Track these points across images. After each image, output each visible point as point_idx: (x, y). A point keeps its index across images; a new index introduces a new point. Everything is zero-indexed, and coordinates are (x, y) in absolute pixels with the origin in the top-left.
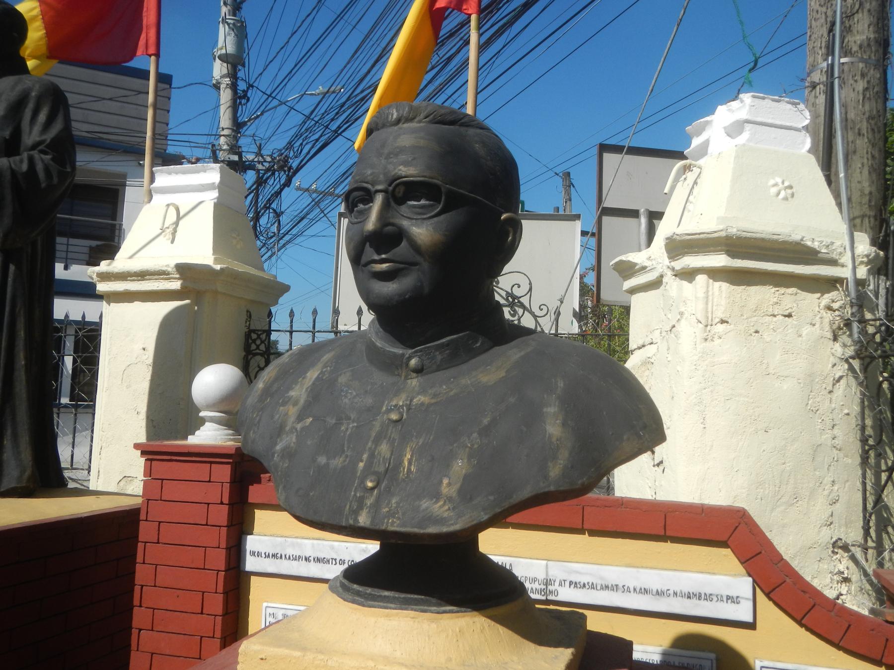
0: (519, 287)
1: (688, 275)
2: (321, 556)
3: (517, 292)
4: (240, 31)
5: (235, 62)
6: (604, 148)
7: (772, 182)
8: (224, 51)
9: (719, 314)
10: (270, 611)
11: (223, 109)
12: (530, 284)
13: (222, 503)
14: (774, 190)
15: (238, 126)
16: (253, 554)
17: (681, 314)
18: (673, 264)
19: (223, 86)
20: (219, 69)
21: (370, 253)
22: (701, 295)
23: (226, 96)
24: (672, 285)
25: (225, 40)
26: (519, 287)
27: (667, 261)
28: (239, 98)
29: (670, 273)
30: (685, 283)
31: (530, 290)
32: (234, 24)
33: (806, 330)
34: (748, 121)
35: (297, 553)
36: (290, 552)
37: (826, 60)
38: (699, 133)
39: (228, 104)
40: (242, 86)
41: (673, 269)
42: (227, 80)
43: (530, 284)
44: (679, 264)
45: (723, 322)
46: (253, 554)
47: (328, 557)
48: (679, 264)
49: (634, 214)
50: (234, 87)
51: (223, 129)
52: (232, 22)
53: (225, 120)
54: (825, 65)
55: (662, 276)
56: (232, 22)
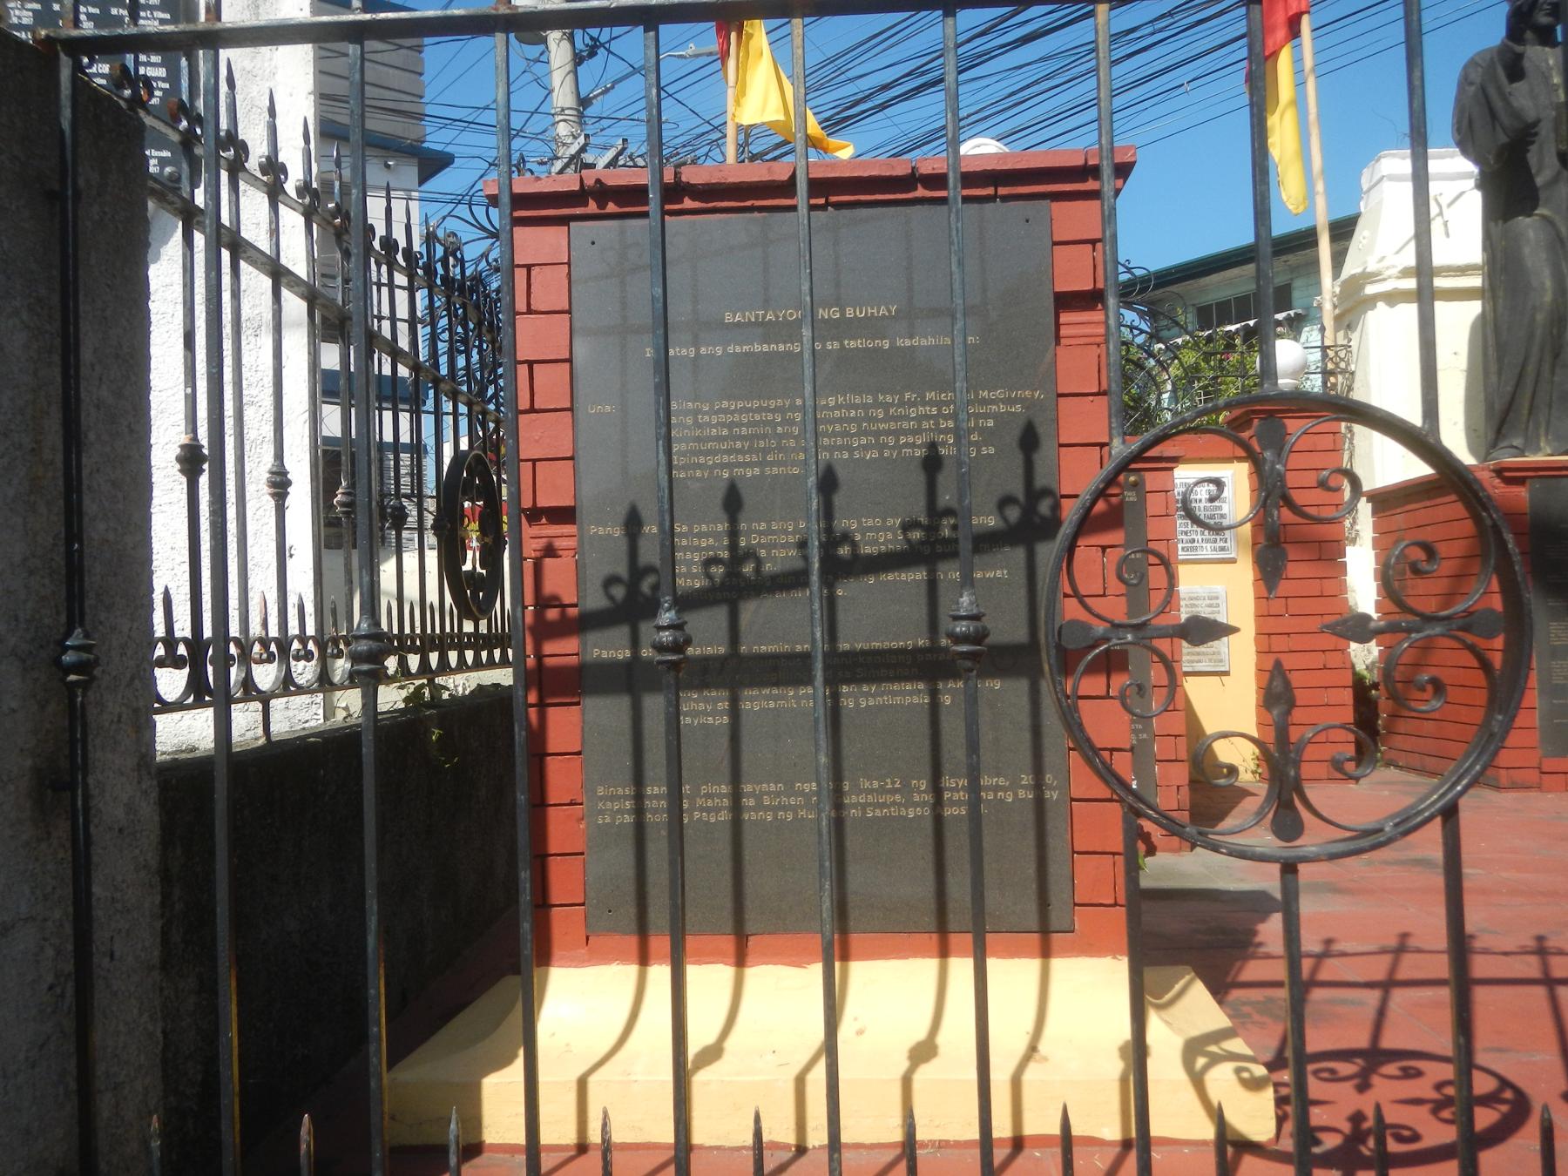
15: (584, 102)
53: (563, 97)
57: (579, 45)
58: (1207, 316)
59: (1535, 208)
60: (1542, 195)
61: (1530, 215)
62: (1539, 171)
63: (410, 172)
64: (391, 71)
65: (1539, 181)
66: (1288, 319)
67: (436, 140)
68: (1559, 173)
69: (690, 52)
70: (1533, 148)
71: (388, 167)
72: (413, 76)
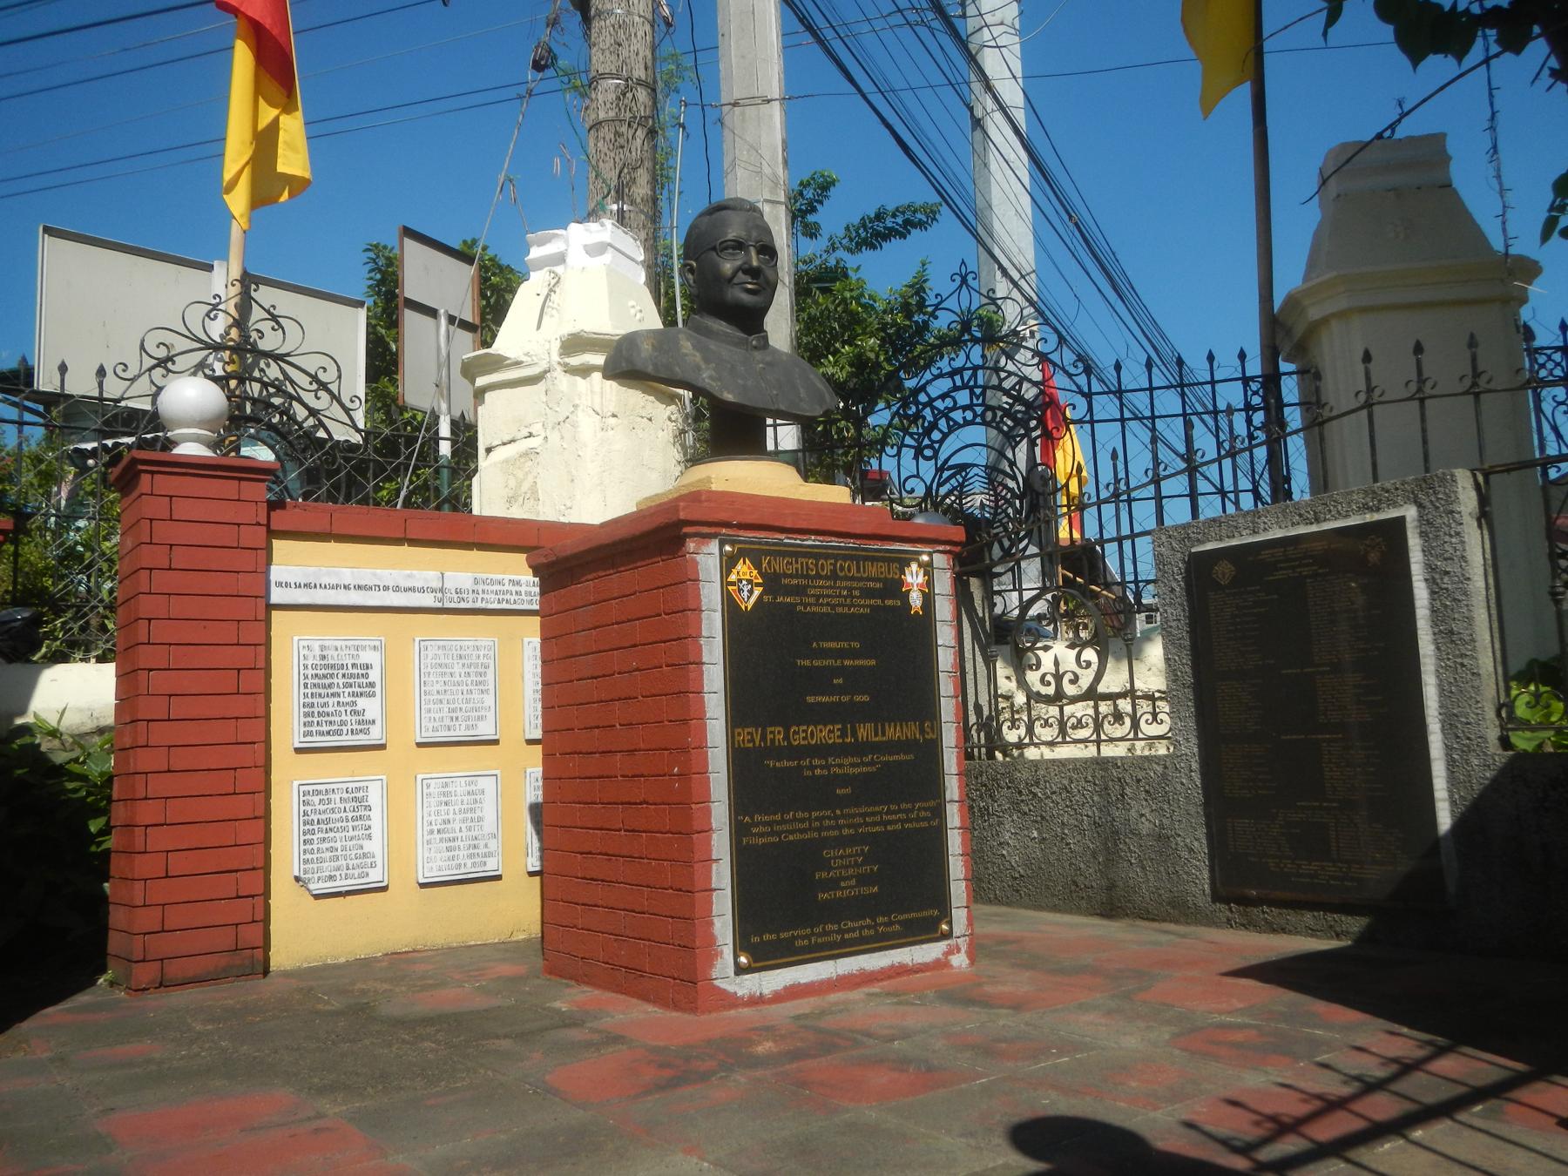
0: (325, 369)
1: (584, 371)
2: (363, 583)
3: (322, 377)
6: (408, 232)
7: (632, 303)
9: (612, 409)
10: (305, 643)
12: (339, 370)
13: (258, 524)
14: (633, 311)
16: (279, 584)
17: (575, 406)
18: (567, 360)
21: (741, 277)
22: (597, 389)
24: (563, 381)
26: (325, 369)
27: (555, 357)
29: (559, 369)
30: (578, 379)
31: (340, 377)
33: (660, 433)
34: (610, 245)
35: (334, 581)
36: (325, 580)
37: (616, 202)
38: (541, 243)
41: (566, 365)
43: (339, 370)
44: (575, 361)
45: (614, 416)
46: (279, 584)
47: (370, 583)
48: (575, 361)
49: (432, 313)
54: (615, 207)
55: (546, 372)
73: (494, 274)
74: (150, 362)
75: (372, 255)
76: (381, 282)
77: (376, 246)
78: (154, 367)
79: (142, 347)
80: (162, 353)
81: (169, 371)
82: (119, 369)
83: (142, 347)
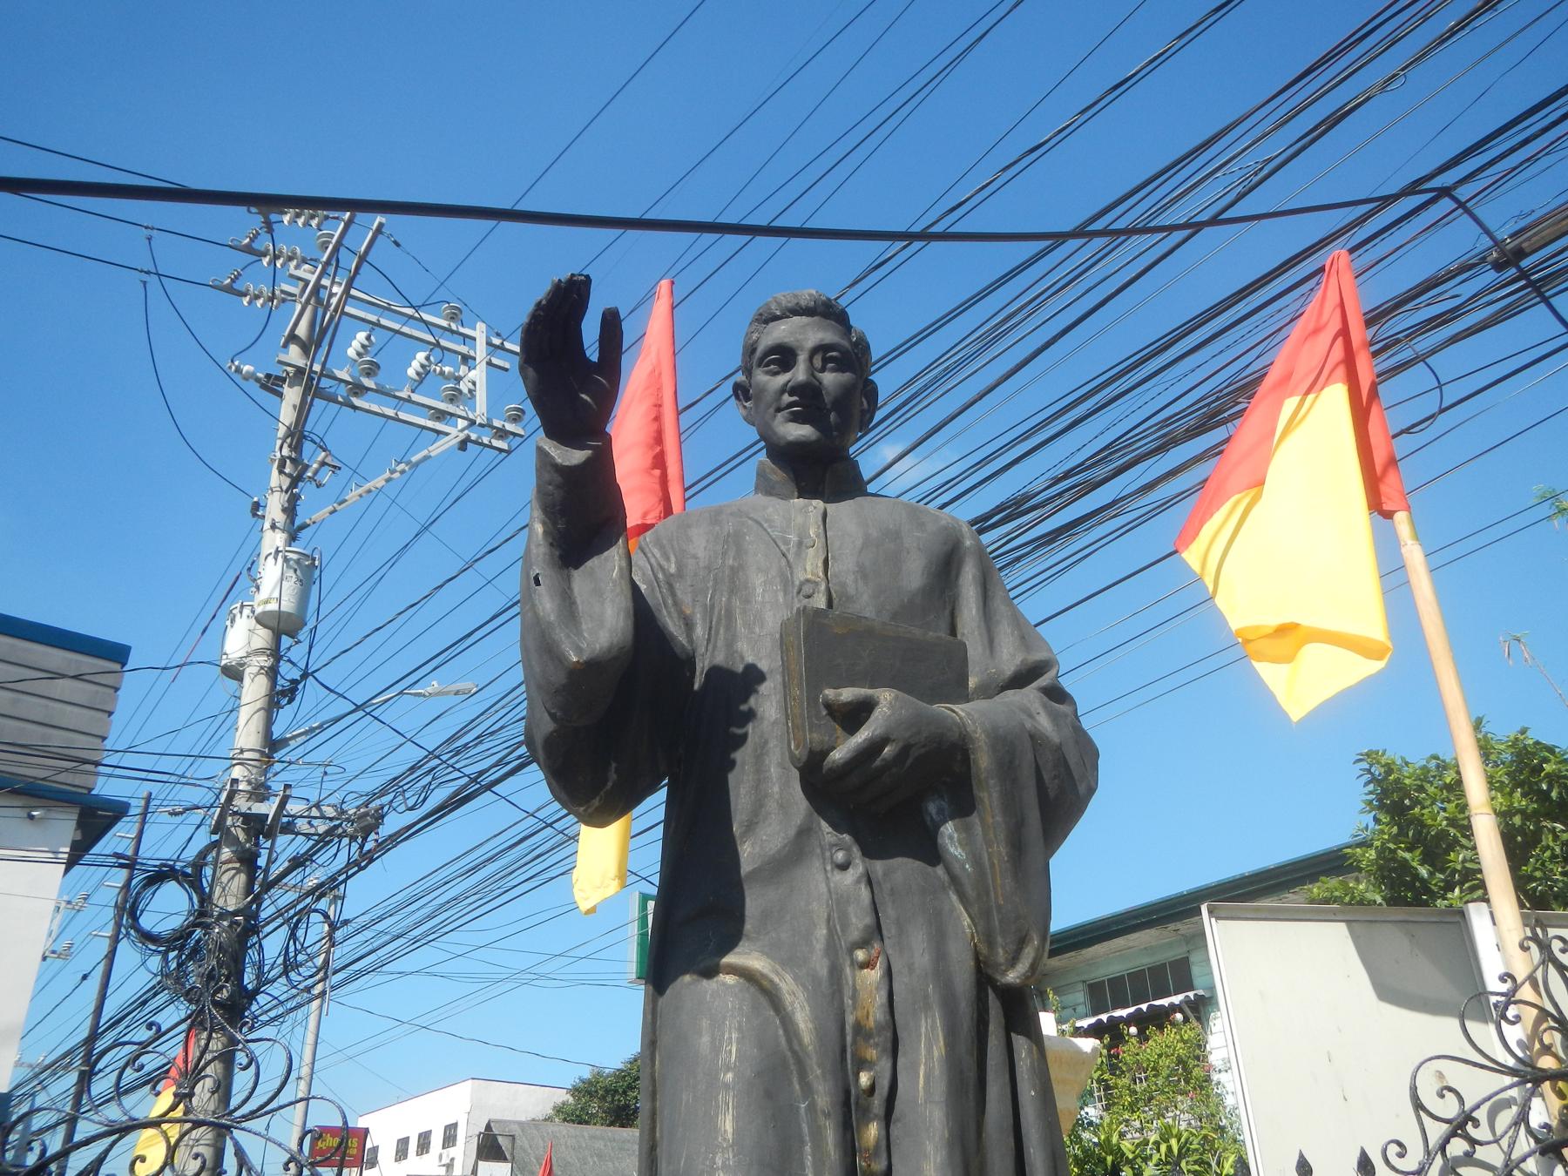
4: (307, 572)
5: (282, 627)
8: (273, 606)
11: (244, 713)
15: (272, 744)
19: (249, 672)
20: (241, 638)
23: (254, 689)
25: (274, 585)
28: (280, 696)
32: (297, 562)
39: (259, 705)
40: (288, 672)
42: (264, 661)
50: (273, 673)
51: (242, 751)
52: (295, 557)
53: (247, 734)
56: (295, 557)
57: (280, 681)
58: (1100, 996)
59: (731, 940)
60: (754, 903)
61: (710, 972)
62: (750, 827)
63: (65, 827)
64: (69, 708)
65: (749, 853)
66: (1187, 1001)
67: (107, 787)
68: (805, 833)
69: (429, 689)
70: (741, 756)
71: (31, 817)
72: (100, 715)
73: (1546, 760)
74: (1436, 1131)
75: (1365, 765)
76: (1385, 793)
77: (1368, 755)
78: (1447, 1141)
79: (1418, 1106)
80: (1449, 1108)
81: (1473, 1142)
82: (1393, 1150)
83: (1418, 1106)
